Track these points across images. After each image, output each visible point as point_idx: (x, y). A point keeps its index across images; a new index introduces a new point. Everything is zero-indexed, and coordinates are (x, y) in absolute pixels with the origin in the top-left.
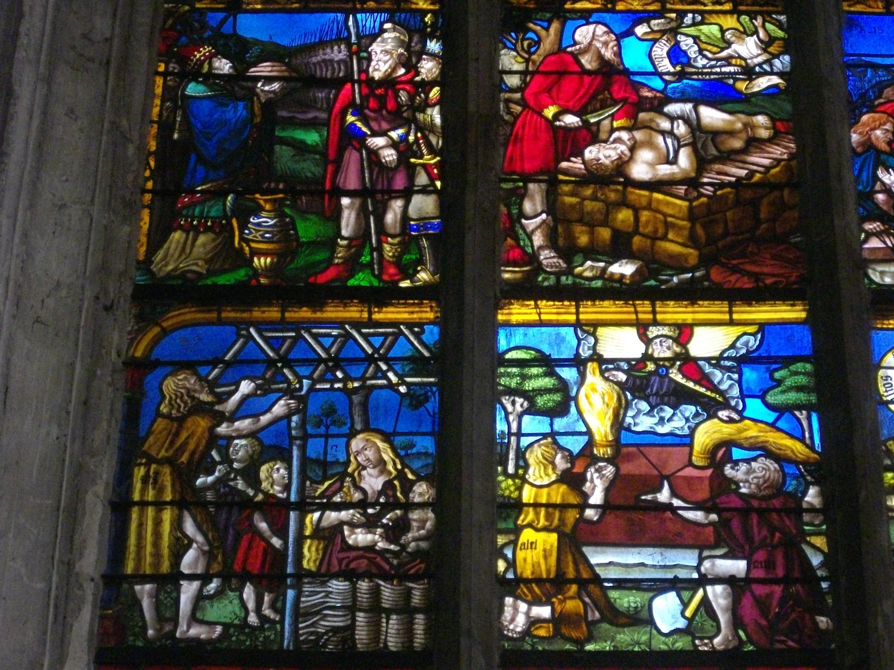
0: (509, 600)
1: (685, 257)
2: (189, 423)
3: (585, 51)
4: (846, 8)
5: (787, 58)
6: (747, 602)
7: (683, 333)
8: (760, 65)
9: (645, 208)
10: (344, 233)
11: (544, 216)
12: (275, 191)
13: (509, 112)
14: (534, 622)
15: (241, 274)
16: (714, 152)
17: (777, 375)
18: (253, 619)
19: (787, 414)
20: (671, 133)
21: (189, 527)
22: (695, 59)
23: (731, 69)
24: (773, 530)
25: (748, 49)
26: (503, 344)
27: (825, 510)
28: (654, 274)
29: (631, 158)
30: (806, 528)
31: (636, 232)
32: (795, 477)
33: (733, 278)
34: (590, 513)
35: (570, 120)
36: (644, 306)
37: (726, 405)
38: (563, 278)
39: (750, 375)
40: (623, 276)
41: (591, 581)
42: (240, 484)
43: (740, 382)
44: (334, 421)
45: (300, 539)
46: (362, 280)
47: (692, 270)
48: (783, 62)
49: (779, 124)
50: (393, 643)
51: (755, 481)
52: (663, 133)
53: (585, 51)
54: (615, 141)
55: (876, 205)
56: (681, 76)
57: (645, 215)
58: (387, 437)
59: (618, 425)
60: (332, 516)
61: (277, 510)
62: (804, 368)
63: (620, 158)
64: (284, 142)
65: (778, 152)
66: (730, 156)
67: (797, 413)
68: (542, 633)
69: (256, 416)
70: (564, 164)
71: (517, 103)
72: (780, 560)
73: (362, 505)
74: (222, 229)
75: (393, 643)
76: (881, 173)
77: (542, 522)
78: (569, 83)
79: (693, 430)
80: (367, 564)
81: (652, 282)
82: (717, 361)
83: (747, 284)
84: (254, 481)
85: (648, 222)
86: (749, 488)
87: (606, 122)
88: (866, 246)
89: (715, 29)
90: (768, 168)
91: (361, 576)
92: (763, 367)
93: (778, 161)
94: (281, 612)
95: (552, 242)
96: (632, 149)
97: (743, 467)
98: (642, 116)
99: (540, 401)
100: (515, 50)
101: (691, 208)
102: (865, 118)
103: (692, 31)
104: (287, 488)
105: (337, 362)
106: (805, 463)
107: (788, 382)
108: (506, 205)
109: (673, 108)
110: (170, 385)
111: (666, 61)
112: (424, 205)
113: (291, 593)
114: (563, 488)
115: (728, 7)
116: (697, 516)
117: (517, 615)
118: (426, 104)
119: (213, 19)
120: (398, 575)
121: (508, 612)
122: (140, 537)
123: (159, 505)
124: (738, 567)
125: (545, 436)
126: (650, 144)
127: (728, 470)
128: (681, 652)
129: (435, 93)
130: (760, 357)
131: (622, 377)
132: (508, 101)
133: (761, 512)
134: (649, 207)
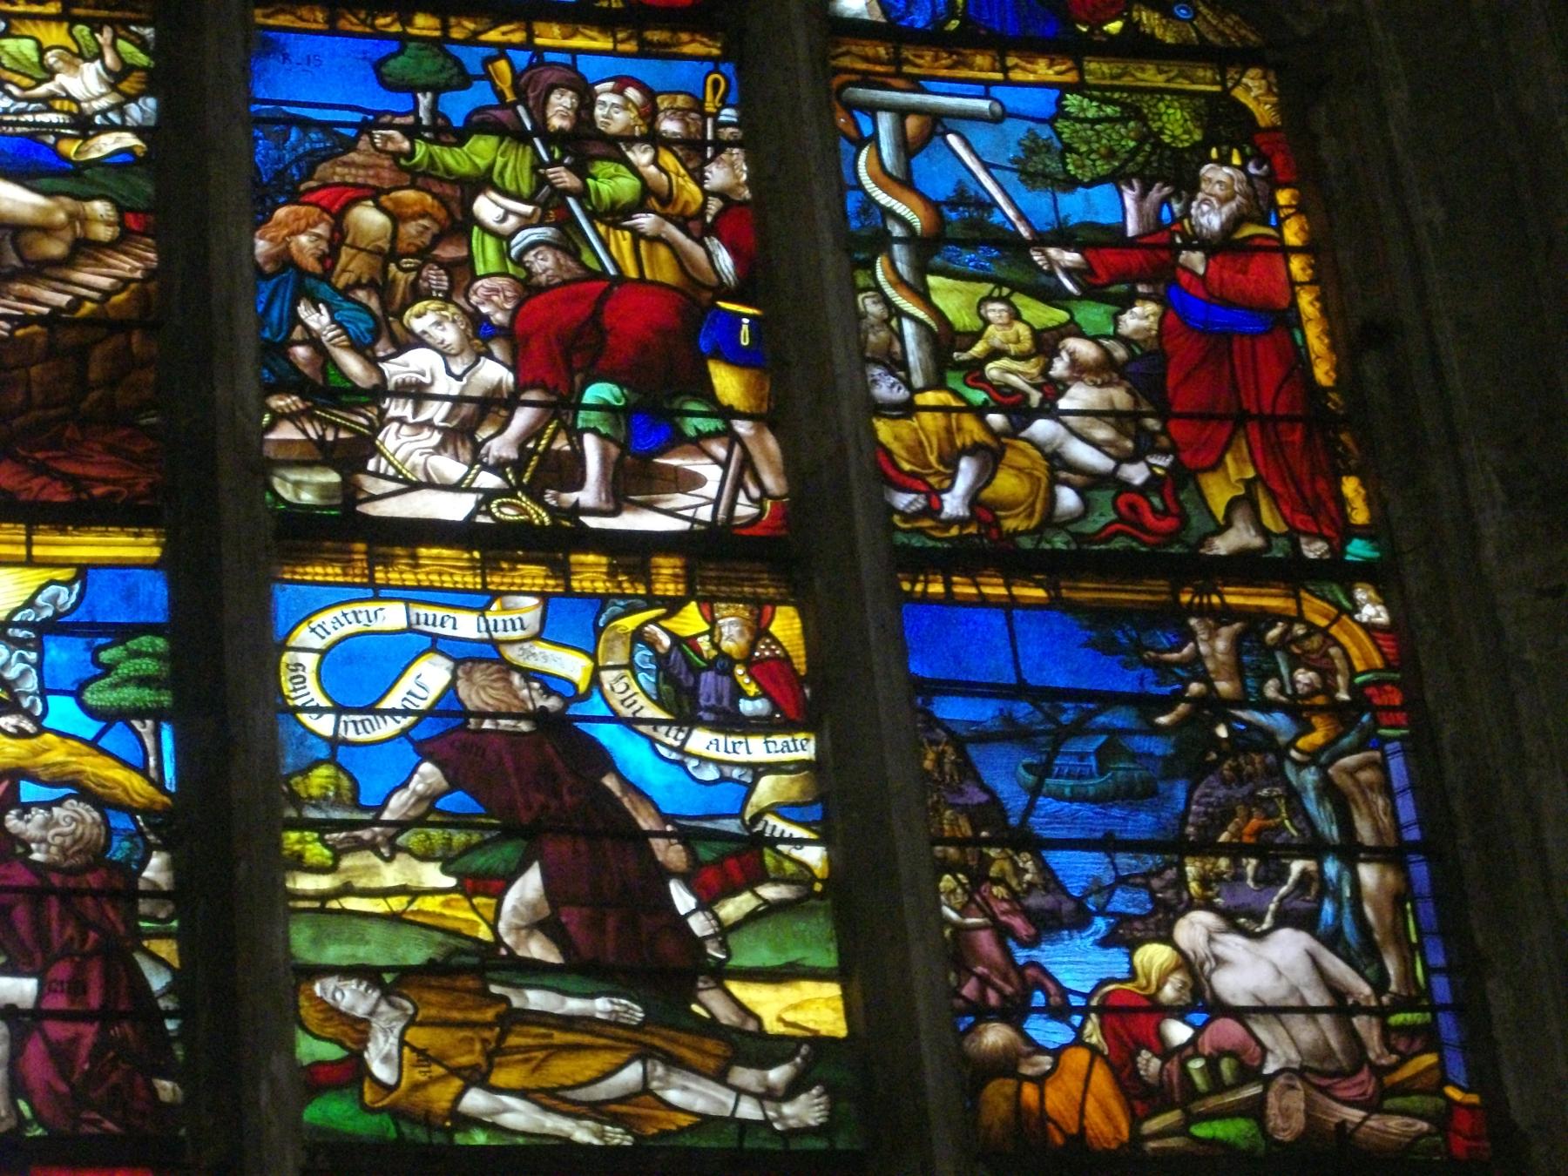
4: (260, 20)
5: (151, 103)
6: (35, 1049)
8: (103, 112)
17: (105, 656)
19: (119, 725)
24: (84, 926)
25: (85, 83)
30: (142, 924)
32: (130, 837)
33: (35, 484)
39: (59, 653)
43: (39, 666)
48: (143, 110)
49: (130, 217)
51: (58, 840)
55: (294, 367)
62: (153, 645)
65: (126, 265)
66: (40, 270)
67: (137, 724)
72: (94, 976)
76: (303, 311)
83: (59, 495)
86: (47, 852)
88: (272, 436)
89: (27, 48)
90: (107, 294)
92: (80, 643)
93: (125, 282)
97: (39, 815)
102: (281, 213)
106: (147, 812)
107: (124, 670)
115: (52, 8)
130: (76, 624)
133: (67, 896)
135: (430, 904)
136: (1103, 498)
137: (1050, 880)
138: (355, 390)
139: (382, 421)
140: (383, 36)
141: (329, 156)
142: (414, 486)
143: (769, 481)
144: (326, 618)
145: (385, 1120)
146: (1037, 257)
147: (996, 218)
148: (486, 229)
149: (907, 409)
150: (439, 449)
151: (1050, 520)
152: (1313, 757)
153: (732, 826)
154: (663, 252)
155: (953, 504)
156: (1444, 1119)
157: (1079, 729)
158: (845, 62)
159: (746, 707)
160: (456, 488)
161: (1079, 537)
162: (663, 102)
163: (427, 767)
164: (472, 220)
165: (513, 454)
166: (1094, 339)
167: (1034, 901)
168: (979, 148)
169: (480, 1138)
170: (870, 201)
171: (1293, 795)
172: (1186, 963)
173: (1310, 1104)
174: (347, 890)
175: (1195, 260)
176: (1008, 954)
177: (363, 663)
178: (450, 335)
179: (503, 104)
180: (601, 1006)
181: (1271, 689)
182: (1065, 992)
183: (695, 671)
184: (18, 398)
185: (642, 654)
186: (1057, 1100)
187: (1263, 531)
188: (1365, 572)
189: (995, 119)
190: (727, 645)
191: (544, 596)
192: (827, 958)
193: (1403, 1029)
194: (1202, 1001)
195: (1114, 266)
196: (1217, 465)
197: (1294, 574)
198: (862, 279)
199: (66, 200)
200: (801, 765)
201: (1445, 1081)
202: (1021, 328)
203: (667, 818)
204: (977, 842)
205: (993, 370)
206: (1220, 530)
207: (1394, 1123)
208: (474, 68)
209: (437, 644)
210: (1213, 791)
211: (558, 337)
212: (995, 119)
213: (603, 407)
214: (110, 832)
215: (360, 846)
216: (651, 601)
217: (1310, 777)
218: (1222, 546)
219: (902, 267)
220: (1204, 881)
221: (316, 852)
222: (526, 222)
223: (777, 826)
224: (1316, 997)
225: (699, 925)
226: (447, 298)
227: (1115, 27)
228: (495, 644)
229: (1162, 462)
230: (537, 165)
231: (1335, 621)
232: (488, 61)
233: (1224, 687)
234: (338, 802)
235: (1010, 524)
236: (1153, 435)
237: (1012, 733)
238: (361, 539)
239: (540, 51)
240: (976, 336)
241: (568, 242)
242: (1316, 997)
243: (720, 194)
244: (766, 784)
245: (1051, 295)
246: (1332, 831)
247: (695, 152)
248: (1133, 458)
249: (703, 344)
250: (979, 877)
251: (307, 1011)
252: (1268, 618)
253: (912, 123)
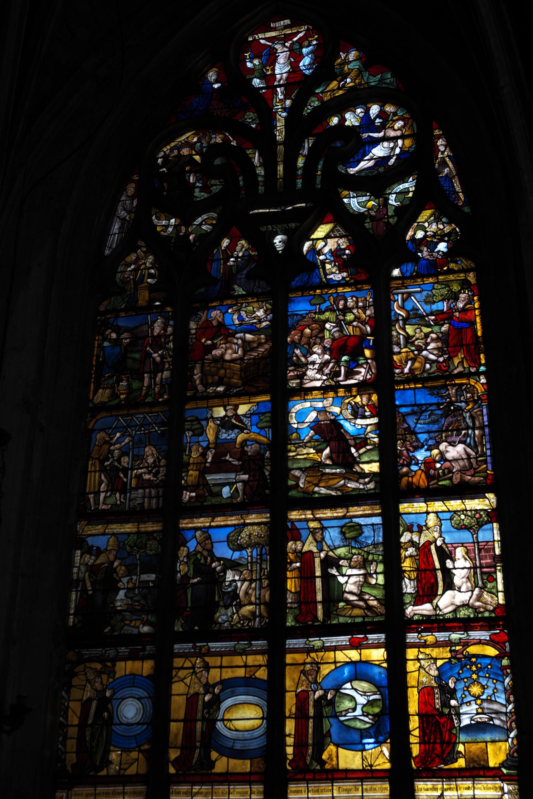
0: (185, 492)
1: (238, 383)
2: (103, 447)
7: (236, 407)
10: (145, 385)
12: (127, 374)
14: (191, 498)
15: (117, 401)
16: (248, 348)
18: (118, 502)
21: (103, 477)
23: (255, 321)
25: (260, 313)
26: (186, 417)
27: (271, 458)
29: (225, 353)
31: (225, 377)
34: (207, 464)
35: (209, 342)
36: (226, 400)
37: (246, 429)
39: (255, 418)
41: (206, 484)
42: (116, 464)
44: (140, 443)
45: (131, 478)
46: (149, 400)
50: (154, 507)
56: (240, 325)
57: (228, 371)
58: (155, 447)
59: (217, 437)
60: (140, 471)
61: (125, 470)
64: (129, 358)
65: (267, 346)
66: (253, 349)
68: (193, 500)
69: (121, 443)
70: (206, 357)
73: (147, 467)
74: (112, 387)
75: (154, 507)
76: (295, 351)
77: (195, 468)
79: (237, 437)
80: (149, 484)
82: (244, 415)
83: (254, 390)
84: (120, 463)
89: (251, 308)
90: (263, 352)
91: (147, 488)
93: (266, 349)
94: (125, 499)
95: (202, 383)
96: (226, 350)
97: (250, 447)
98: (229, 339)
99: (196, 432)
101: (241, 367)
104: (128, 464)
105: (142, 425)
106: (267, 444)
109: (238, 335)
110: (98, 436)
112: (166, 374)
113: (128, 494)
114: (201, 458)
115: (255, 300)
116: (236, 463)
117: (187, 495)
118: (169, 342)
119: (111, 320)
120: (156, 487)
121: (184, 495)
122: (90, 481)
123: (95, 471)
124: (245, 477)
125: (196, 442)
126: (231, 348)
127: (246, 448)
128: (229, 504)
129: (171, 338)
131: (219, 422)
132: (192, 338)
134: (229, 368)
135: (311, 456)
136: (434, 365)
137: (418, 440)
138: (303, 364)
139: (307, 369)
140: (311, 295)
141: (301, 320)
142: (312, 381)
143: (373, 371)
144: (297, 407)
145: (302, 494)
146: (427, 319)
147: (420, 312)
148: (327, 330)
149: (400, 353)
150: (316, 373)
151: (424, 371)
152: (469, 411)
153: (363, 436)
154: (358, 329)
155: (406, 370)
156: (486, 478)
157: (426, 411)
158: (393, 285)
159: (367, 414)
160: (319, 380)
161: (429, 374)
162: (360, 300)
163: (312, 431)
164: (325, 328)
165: (328, 372)
166: (436, 333)
167: (414, 444)
168: (417, 298)
169: (317, 495)
170: (396, 312)
171: (464, 418)
172: (441, 453)
173: (461, 476)
174: (298, 455)
175: (457, 314)
176: (408, 454)
177: (304, 413)
178: (319, 351)
179: (332, 305)
180: (338, 470)
181: (462, 399)
182: (418, 460)
183: (358, 408)
185: (349, 406)
186: (415, 480)
187: (464, 368)
188: (483, 373)
189: (420, 292)
190: (364, 403)
191: (333, 398)
192: (377, 458)
193: (480, 461)
194: (443, 458)
195: (441, 317)
196: (457, 355)
197: (469, 375)
198: (393, 328)
200: (375, 424)
201: (487, 470)
202: (422, 334)
203: (352, 436)
204: (405, 434)
205: (416, 343)
206: (456, 368)
207: (477, 479)
208: (326, 299)
209: (315, 409)
210: (449, 419)
211: (337, 350)
212: (420, 292)
213: (345, 361)
214: (261, 448)
215: (300, 447)
216: (351, 396)
217: (468, 414)
218: (456, 372)
219: (401, 325)
220: (446, 437)
221: (293, 448)
222: (334, 327)
223: (371, 435)
224: (464, 456)
225: (356, 455)
226: (320, 344)
227: (445, 268)
228: (324, 407)
229: (446, 356)
230: (337, 315)
231: (476, 383)
232: (329, 297)
233: (453, 399)
234: (297, 439)
235: (416, 373)
236: (445, 351)
237: (413, 413)
238: (303, 392)
239: (338, 293)
240: (414, 336)
241: (341, 330)
242: (464, 456)
243: (369, 316)
244: (369, 428)
245: (428, 326)
246: (471, 424)
247: (364, 309)
248: (440, 357)
249: (364, 346)
250: (405, 441)
251: (290, 477)
252: (463, 384)
253: (405, 296)
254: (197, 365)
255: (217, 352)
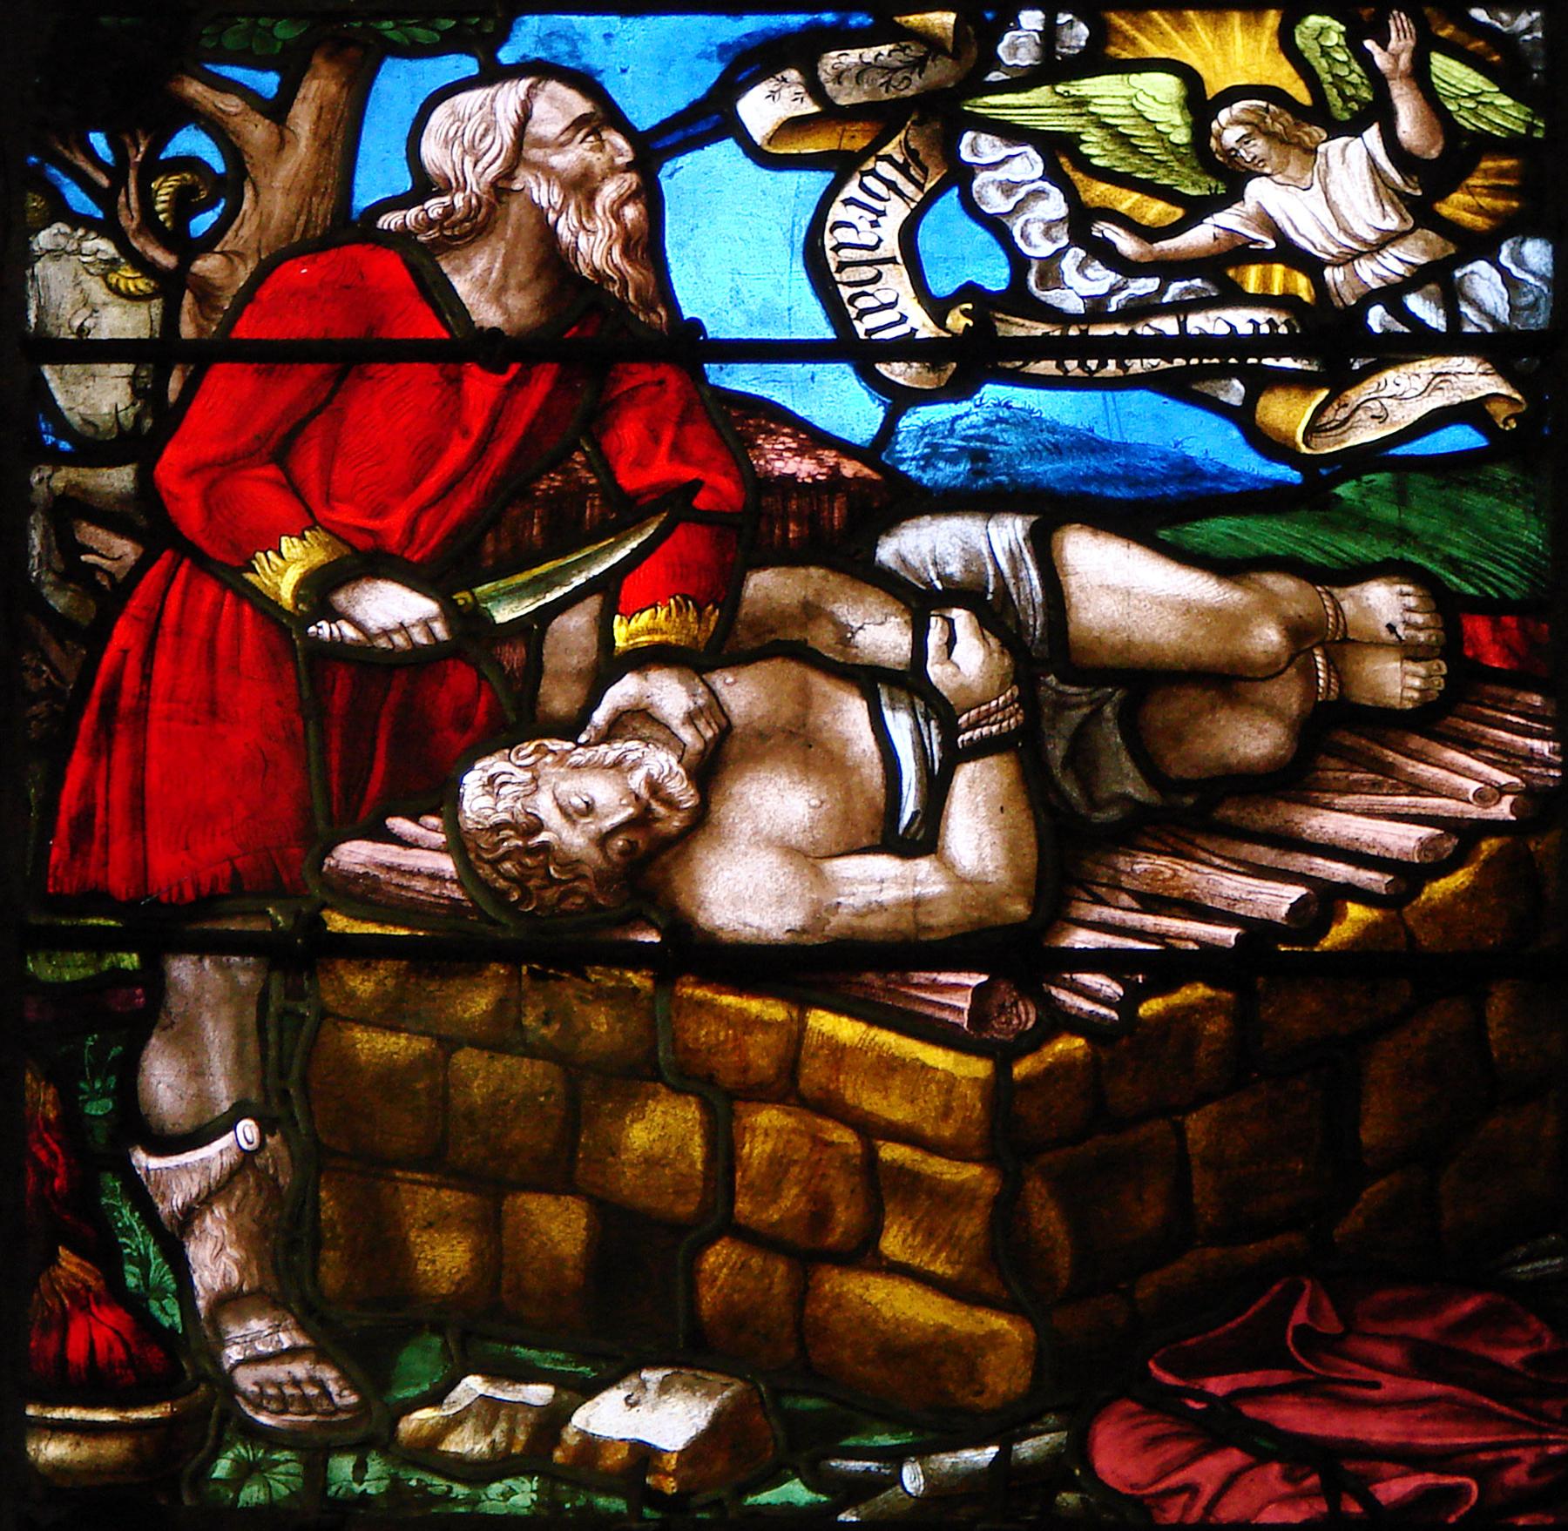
1: (962, 1353)
3: (477, 226)
5: (1537, 253)
8: (1391, 295)
9: (762, 1094)
11: (247, 1130)
13: (77, 574)
16: (1134, 787)
20: (909, 680)
22: (1050, 271)
23: (1241, 320)
25: (1332, 202)
28: (805, 1451)
29: (701, 820)
33: (1210, 1470)
35: (391, 608)
38: (343, 1467)
40: (643, 1454)
47: (1004, 1427)
49: (1478, 628)
52: (870, 680)
53: (477, 226)
54: (617, 728)
57: (767, 1129)
63: (642, 820)
65: (1467, 783)
70: (355, 854)
71: (113, 518)
78: (393, 404)
81: (796, 1492)
85: (778, 1165)
87: (576, 624)
90: (1409, 874)
93: (1466, 833)
96: (710, 769)
98: (768, 586)
100: (109, 228)
101: (999, 1090)
103: (1038, 107)
108: (50, 1077)
109: (928, 544)
111: (896, 282)
126: (801, 744)
132: (72, 509)
134: (785, 1085)
184: (1149, 1212)
199: (1282, 584)
254: (182, 970)
255: (557, 795)
